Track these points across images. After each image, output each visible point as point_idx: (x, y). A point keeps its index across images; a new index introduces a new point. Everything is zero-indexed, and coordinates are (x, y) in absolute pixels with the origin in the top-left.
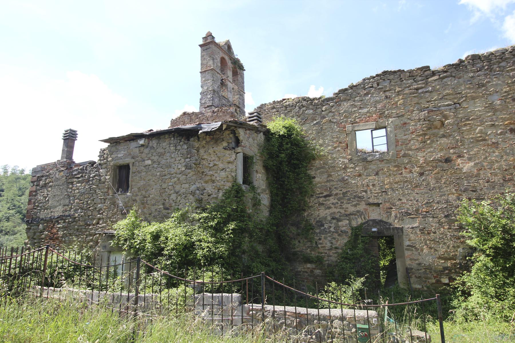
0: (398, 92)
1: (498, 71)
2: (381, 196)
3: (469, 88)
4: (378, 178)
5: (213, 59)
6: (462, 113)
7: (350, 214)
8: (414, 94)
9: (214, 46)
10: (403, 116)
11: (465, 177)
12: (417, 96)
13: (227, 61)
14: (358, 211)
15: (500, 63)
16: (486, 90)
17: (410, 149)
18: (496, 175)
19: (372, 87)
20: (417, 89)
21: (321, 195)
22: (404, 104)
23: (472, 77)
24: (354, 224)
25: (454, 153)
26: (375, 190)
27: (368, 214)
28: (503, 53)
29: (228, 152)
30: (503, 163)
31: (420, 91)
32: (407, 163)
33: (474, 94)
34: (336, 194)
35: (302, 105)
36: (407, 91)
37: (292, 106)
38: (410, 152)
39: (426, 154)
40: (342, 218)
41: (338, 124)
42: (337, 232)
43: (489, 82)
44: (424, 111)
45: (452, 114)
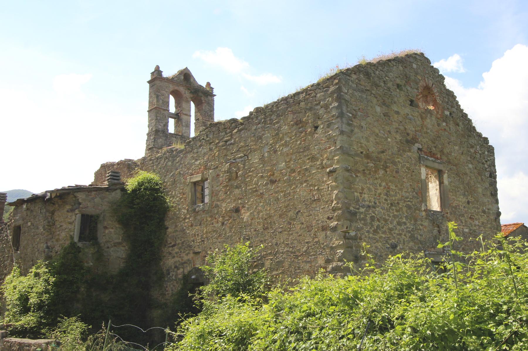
0: (216, 144)
1: (269, 124)
2: (201, 245)
3: (253, 141)
4: (201, 228)
5: (157, 97)
6: (248, 165)
7: (185, 263)
8: (224, 146)
9: (159, 82)
10: (217, 167)
11: (245, 226)
12: (226, 148)
13: (183, 93)
14: (189, 260)
15: (272, 115)
16: (261, 143)
17: (218, 200)
18: (260, 225)
19: (203, 139)
20: (226, 142)
21: (170, 245)
22: (218, 156)
23: (255, 130)
24: (186, 272)
25: (241, 204)
26: (198, 240)
27: (194, 262)
28: (273, 106)
29: (70, 214)
30: (264, 212)
31: (228, 143)
32: (217, 213)
33: (254, 147)
34: (179, 244)
35: (166, 157)
36: (221, 144)
37: (161, 158)
38: (218, 202)
39: (226, 204)
40: (180, 266)
41: (184, 175)
42: (176, 280)
43: (263, 135)
44: (228, 163)
45: (242, 166)
